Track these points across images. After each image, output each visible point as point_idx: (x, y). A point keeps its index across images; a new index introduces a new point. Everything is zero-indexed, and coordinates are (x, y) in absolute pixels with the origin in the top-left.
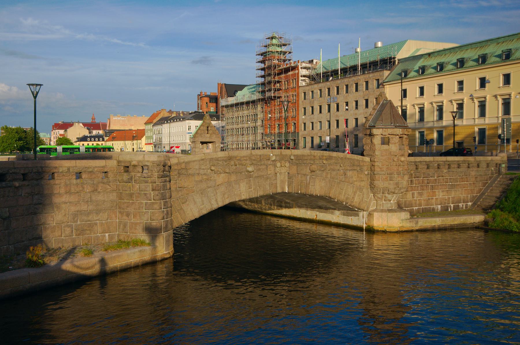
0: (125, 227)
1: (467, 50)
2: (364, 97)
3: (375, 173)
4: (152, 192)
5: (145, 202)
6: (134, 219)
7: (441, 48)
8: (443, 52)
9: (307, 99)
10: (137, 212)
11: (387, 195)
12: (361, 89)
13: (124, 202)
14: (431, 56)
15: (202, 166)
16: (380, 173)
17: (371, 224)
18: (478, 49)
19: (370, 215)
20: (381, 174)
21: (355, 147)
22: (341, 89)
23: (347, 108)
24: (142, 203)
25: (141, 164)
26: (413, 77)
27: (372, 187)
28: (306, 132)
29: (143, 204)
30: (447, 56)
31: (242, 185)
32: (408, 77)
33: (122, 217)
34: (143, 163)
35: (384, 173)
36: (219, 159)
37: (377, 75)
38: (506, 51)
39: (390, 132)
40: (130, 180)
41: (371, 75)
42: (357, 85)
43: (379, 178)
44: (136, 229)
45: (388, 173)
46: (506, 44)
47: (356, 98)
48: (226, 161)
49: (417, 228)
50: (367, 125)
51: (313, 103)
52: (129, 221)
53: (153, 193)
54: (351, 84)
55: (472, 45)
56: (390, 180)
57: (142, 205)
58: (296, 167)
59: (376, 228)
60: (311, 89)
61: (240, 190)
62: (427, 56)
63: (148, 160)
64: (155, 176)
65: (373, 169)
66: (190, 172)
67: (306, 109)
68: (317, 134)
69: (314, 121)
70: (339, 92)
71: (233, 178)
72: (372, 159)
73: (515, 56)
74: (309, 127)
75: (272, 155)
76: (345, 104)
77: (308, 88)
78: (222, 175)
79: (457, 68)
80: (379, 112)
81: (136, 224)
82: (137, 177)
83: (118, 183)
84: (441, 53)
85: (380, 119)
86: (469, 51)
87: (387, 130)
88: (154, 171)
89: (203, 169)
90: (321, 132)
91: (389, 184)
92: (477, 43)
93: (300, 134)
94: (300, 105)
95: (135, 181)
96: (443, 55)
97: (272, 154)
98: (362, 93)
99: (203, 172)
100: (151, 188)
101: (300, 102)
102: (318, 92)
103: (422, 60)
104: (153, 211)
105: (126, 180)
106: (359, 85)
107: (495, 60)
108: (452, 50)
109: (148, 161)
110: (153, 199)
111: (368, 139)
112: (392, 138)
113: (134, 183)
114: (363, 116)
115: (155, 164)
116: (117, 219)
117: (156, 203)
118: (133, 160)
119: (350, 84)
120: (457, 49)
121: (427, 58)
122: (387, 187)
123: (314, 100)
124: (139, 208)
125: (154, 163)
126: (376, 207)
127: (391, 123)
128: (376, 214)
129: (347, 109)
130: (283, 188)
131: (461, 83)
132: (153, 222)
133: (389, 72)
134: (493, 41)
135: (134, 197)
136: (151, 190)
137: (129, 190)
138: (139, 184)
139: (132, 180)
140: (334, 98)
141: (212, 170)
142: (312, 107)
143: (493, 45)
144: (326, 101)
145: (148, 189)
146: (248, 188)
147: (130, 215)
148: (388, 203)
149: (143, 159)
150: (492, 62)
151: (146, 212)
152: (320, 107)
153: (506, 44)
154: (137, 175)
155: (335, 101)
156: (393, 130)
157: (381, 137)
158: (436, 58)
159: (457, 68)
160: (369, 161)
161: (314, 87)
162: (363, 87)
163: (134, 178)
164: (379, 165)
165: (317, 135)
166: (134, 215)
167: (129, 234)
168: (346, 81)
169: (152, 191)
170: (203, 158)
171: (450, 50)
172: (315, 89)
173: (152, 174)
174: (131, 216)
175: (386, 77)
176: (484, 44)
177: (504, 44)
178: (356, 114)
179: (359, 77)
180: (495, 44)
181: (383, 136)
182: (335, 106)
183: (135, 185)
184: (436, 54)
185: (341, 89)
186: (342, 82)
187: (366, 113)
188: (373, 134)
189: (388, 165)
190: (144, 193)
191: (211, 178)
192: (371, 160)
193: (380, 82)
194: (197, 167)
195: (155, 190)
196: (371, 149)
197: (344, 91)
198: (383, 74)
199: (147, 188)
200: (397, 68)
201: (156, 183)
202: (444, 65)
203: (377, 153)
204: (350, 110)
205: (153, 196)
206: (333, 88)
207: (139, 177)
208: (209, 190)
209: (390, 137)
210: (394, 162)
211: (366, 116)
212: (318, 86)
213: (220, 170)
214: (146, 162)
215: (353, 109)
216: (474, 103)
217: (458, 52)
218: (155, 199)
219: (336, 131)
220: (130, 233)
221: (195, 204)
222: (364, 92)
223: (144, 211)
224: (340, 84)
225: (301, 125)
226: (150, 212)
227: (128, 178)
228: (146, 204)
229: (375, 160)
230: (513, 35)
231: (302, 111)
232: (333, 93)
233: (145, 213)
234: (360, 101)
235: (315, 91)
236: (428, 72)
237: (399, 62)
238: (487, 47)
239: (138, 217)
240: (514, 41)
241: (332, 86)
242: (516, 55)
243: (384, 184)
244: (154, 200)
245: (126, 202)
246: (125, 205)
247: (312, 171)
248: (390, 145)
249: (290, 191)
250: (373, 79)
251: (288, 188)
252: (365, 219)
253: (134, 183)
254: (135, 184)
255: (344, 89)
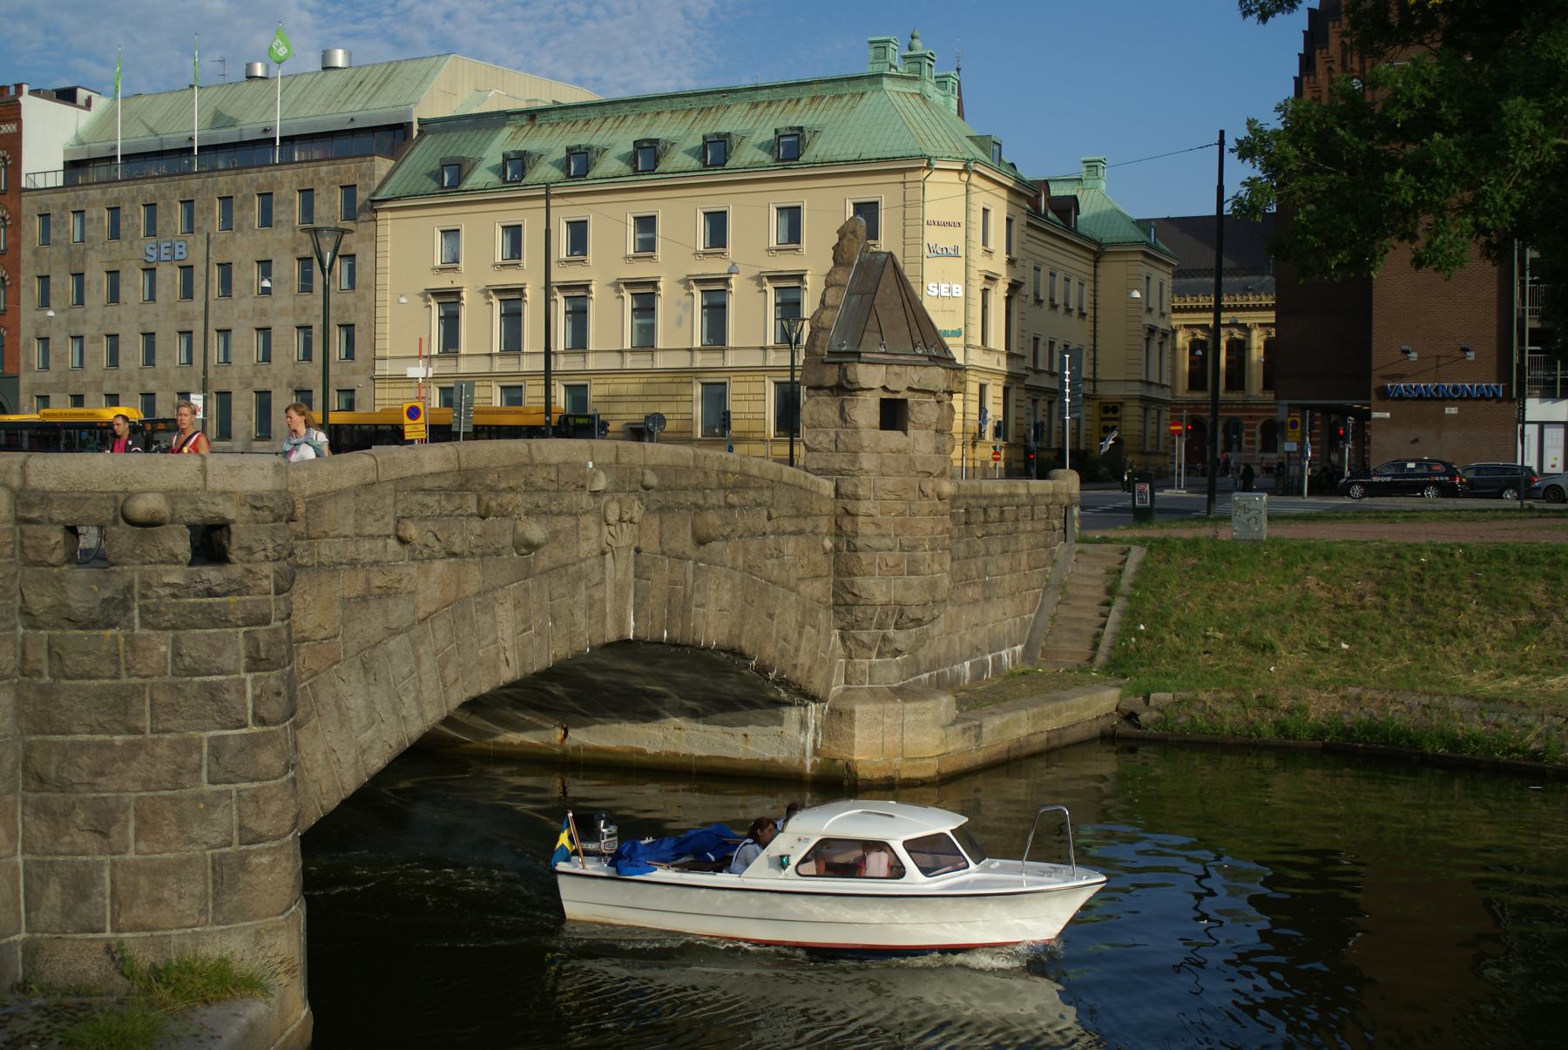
0: (84, 896)
1: (658, 113)
2: (294, 250)
3: (859, 543)
4: (249, 677)
5: (210, 739)
6: (142, 846)
7: (544, 101)
8: (579, 112)
9: (56, 243)
10: (165, 798)
11: (891, 633)
12: (283, 217)
13: (73, 743)
14: (537, 122)
15: (370, 519)
16: (874, 542)
17: (839, 753)
18: (695, 114)
19: (839, 716)
20: (878, 550)
21: (258, 439)
22: (201, 211)
23: (266, 284)
24: (191, 746)
25: (187, 512)
26: (483, 190)
27: (845, 602)
28: (49, 377)
29: (200, 748)
30: (593, 126)
31: (500, 611)
32: (467, 185)
33: (56, 838)
34: (201, 505)
35: (888, 542)
36: (428, 484)
37: (348, 170)
38: (788, 133)
39: (916, 378)
40: (113, 611)
41: (324, 169)
42: (266, 198)
43: (872, 564)
44: (157, 902)
45: (905, 543)
46: (780, 109)
47: (265, 252)
48: (447, 492)
49: (979, 757)
50: (823, 348)
51: (83, 260)
52: (107, 859)
53: (255, 680)
54: (245, 197)
55: (675, 100)
56: (910, 573)
57: (195, 757)
58: (657, 521)
59: (863, 773)
60: (74, 204)
61: (495, 642)
62: (523, 121)
63: (229, 488)
64: (265, 583)
65: (847, 524)
66: (323, 551)
67: (53, 280)
68: (98, 384)
69: (88, 331)
70: (196, 225)
71: (474, 577)
72: (846, 487)
73: (813, 153)
74: (62, 358)
75: (591, 465)
76: (256, 271)
77: (59, 198)
78: (439, 566)
79: (636, 171)
80: (855, 299)
81: (158, 872)
82: (162, 592)
83: (21, 630)
84: (571, 115)
85: (872, 323)
86: (665, 117)
87: (903, 368)
88: (260, 556)
89: (371, 537)
90: (118, 379)
91: (907, 587)
92: (689, 95)
93: (25, 381)
94: (22, 265)
95: (149, 617)
96: (581, 123)
97: (592, 460)
98: (290, 235)
99: (371, 551)
100: (243, 653)
101: (26, 254)
102: (103, 218)
103: (507, 131)
104: (256, 785)
105: (90, 610)
106: (278, 202)
107: (756, 159)
108: (609, 110)
109: (225, 494)
110: (255, 715)
111: (827, 404)
112: (919, 404)
113: (144, 624)
114: (291, 321)
115: (267, 513)
116: (15, 854)
117: (270, 739)
118: (137, 487)
119: (240, 195)
120: (626, 108)
121: (522, 126)
122: (899, 598)
123: (85, 250)
124: (177, 774)
125: (259, 504)
126: (846, 682)
127: (915, 347)
128: (863, 711)
129: (267, 291)
130: (621, 622)
131: (646, 224)
132: (260, 853)
133: (391, 163)
134: (739, 95)
135: (142, 713)
136: (243, 662)
137: (108, 668)
138: (170, 634)
139: (128, 609)
140: (172, 247)
141: (402, 541)
142: (79, 276)
143: (738, 107)
144: (140, 255)
145: (227, 660)
146: (521, 627)
147: (116, 821)
148: (887, 663)
149: (200, 483)
150: (746, 164)
151: (220, 794)
152: (114, 275)
153: (780, 109)
154: (166, 580)
155: (177, 257)
156: (925, 370)
157: (882, 400)
158: (558, 130)
159: (636, 171)
160: (833, 495)
161: (86, 196)
162: (293, 212)
163: (144, 596)
164: (873, 511)
165: (99, 390)
166: (142, 819)
167: (108, 934)
168: (224, 182)
169: (248, 670)
170: (371, 476)
171: (602, 108)
172: (92, 204)
173: (250, 571)
174: (126, 826)
175: (381, 179)
176: (709, 101)
177: (773, 108)
178: (264, 313)
179: (278, 174)
180: (746, 107)
181: (886, 396)
182: (174, 276)
183: (147, 638)
184: (555, 116)
185: (201, 211)
186: (207, 188)
187: (304, 309)
188: (856, 386)
189: (903, 514)
190: (204, 684)
191: (400, 581)
192: (842, 490)
193: (362, 196)
194: (348, 527)
195: (263, 665)
196: (841, 446)
197: (214, 221)
198: (372, 169)
199: (219, 653)
200: (417, 150)
201: (268, 623)
202: (592, 156)
203: (867, 462)
204: (240, 297)
205: (257, 698)
206: (169, 206)
207: (177, 591)
208: (392, 644)
209: (912, 399)
210: (925, 502)
211: (303, 322)
212: (104, 193)
213: (431, 540)
214: (219, 500)
215: (252, 293)
216: (690, 297)
217: (630, 119)
218: (265, 715)
219: (182, 376)
220: (117, 929)
221: (342, 726)
222: (294, 230)
223: (207, 788)
224: (198, 191)
225: (29, 345)
226: (239, 791)
227: (107, 594)
228: (217, 747)
229: (861, 492)
230: (798, 84)
231: (33, 291)
232: (168, 224)
233: (211, 803)
234: (278, 263)
235: (126, 209)
236: (537, 176)
237: (424, 128)
238: (721, 112)
239: (170, 832)
240: (802, 103)
241: (163, 196)
242: (816, 149)
243: (889, 591)
244: (260, 720)
245: (84, 746)
246: (84, 760)
247: (701, 541)
248: (911, 431)
249: (641, 635)
250: (334, 183)
251: (635, 620)
252: (810, 736)
253: (144, 624)
254: (146, 632)
255: (214, 209)
